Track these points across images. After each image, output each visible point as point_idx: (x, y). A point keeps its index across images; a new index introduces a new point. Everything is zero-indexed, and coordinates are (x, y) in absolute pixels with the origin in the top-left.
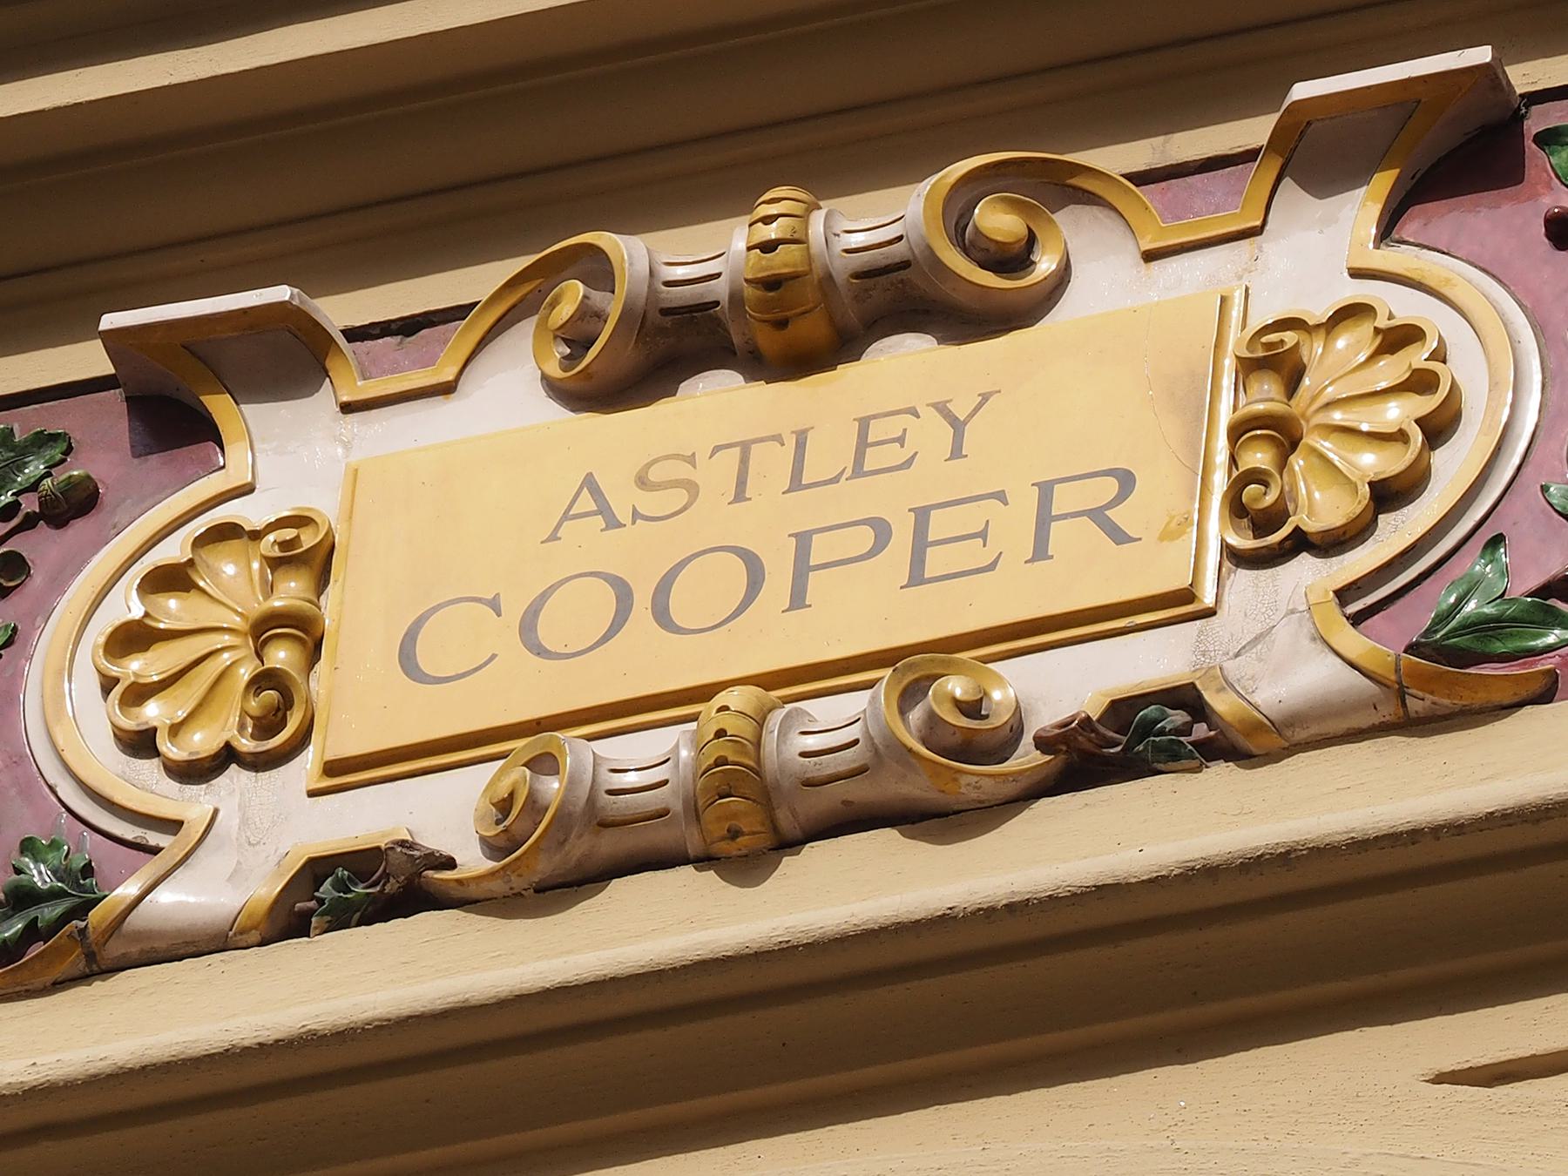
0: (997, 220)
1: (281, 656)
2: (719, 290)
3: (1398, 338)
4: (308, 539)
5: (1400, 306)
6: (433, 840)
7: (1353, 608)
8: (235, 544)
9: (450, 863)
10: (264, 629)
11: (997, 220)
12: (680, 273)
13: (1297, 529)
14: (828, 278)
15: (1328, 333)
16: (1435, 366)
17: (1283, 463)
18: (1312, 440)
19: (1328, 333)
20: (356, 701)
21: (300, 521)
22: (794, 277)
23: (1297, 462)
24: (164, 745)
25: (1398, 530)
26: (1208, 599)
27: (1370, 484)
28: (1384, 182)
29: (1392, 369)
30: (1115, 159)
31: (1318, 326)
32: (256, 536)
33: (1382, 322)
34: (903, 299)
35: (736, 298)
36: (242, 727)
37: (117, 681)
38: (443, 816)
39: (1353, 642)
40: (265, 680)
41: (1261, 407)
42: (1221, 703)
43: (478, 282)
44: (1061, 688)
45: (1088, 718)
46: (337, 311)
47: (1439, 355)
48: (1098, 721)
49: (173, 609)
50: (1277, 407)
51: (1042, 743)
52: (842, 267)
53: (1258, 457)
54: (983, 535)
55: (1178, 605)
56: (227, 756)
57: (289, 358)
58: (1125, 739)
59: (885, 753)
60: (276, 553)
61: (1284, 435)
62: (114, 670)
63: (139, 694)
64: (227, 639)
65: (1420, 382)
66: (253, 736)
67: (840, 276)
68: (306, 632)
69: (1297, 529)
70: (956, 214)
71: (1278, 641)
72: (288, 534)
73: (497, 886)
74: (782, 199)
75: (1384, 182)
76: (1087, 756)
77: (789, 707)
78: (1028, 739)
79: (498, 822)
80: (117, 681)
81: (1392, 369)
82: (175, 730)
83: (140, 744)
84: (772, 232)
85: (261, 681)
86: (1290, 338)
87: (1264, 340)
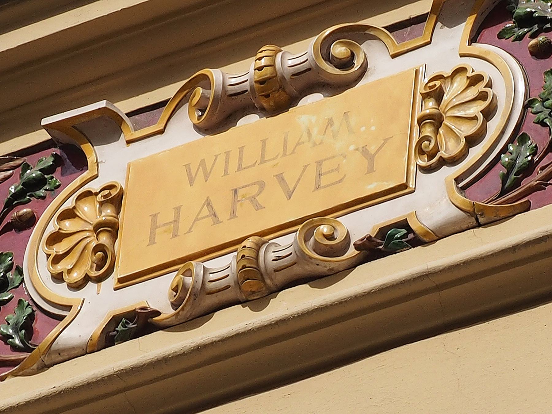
0: (339, 50)
1: (104, 239)
2: (246, 86)
3: (476, 80)
4: (114, 193)
5: (476, 66)
6: (153, 306)
7: (460, 185)
8: (90, 198)
9: (158, 313)
10: (98, 228)
11: (339, 50)
12: (233, 81)
13: (441, 157)
14: (283, 78)
15: (452, 79)
16: (487, 89)
17: (437, 132)
18: (446, 122)
19: (452, 79)
20: (129, 255)
21: (111, 187)
22: (270, 78)
23: (441, 131)
24: (66, 276)
25: (476, 153)
26: (411, 185)
27: (465, 137)
28: (471, 20)
29: (473, 92)
30: (379, 21)
31: (448, 77)
32: (97, 194)
33: (470, 74)
34: (310, 82)
35: (252, 87)
36: (92, 267)
37: (50, 255)
38: (156, 295)
39: (459, 198)
40: (99, 248)
41: (428, 111)
42: (413, 225)
43: (169, 91)
44: (361, 225)
45: (370, 236)
46: (123, 107)
47: (489, 85)
48: (375, 237)
49: (68, 226)
50: (435, 111)
51: (357, 247)
52: (288, 72)
53: (428, 131)
54: (337, 169)
55: (401, 189)
56: (87, 279)
57: (108, 127)
58: (384, 242)
59: (302, 257)
60: (103, 199)
61: (436, 121)
62: (49, 252)
63: (57, 259)
64: (88, 234)
65: (482, 96)
66: (96, 270)
67: (287, 77)
68: (112, 228)
69: (441, 157)
70: (324, 50)
71: (433, 200)
72: (106, 192)
73: (174, 321)
74: (267, 49)
75: (471, 20)
76: (370, 250)
77: (271, 242)
78: (352, 248)
79: (175, 296)
80: (50, 255)
81: (473, 92)
82: (69, 271)
83: (58, 278)
84: (263, 62)
85: (97, 249)
86: (438, 83)
87: (429, 85)
